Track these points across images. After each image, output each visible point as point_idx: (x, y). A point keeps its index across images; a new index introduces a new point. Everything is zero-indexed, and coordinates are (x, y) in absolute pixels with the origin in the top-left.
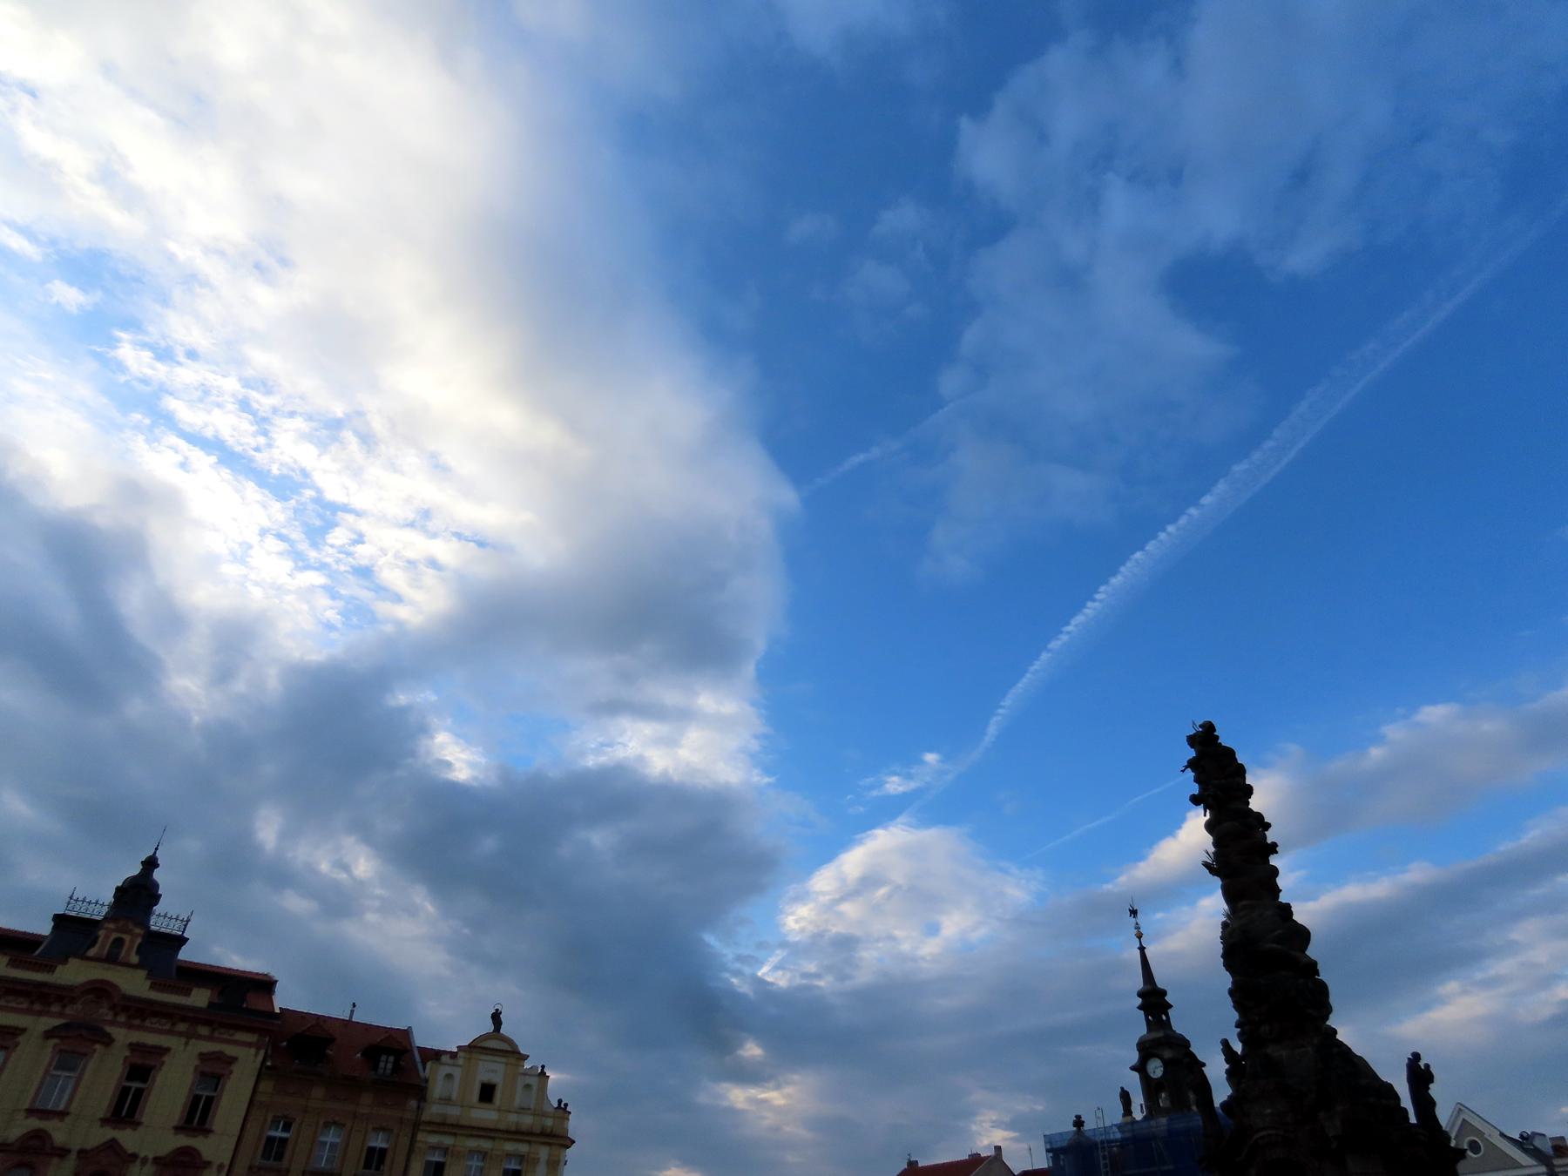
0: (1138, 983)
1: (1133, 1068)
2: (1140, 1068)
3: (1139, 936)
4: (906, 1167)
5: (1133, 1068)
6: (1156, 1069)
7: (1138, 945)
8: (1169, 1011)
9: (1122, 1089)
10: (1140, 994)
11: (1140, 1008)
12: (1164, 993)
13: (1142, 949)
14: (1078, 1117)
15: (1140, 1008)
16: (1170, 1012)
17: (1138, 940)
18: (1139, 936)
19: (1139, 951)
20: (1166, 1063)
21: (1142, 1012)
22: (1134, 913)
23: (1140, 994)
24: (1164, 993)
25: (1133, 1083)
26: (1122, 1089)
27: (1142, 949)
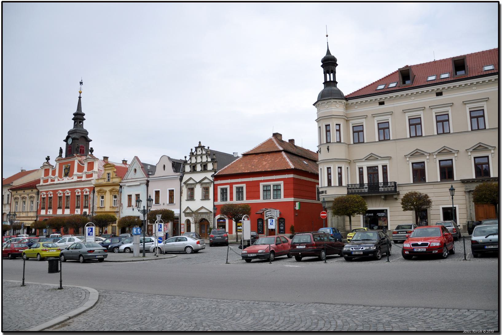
0: (75, 111)
1: (64, 141)
2: (66, 141)
3: (80, 93)
4: (21, 172)
5: (64, 141)
6: (70, 141)
7: (79, 96)
8: (84, 121)
9: (61, 148)
10: (74, 114)
11: (73, 119)
12: (84, 115)
13: (80, 97)
14: (48, 157)
15: (73, 119)
16: (84, 121)
17: (79, 94)
18: (80, 93)
19: (79, 98)
20: (73, 139)
21: (73, 121)
22: (81, 83)
23: (74, 114)
24: (84, 115)
25: (64, 146)
26: (61, 148)
27: (80, 97)
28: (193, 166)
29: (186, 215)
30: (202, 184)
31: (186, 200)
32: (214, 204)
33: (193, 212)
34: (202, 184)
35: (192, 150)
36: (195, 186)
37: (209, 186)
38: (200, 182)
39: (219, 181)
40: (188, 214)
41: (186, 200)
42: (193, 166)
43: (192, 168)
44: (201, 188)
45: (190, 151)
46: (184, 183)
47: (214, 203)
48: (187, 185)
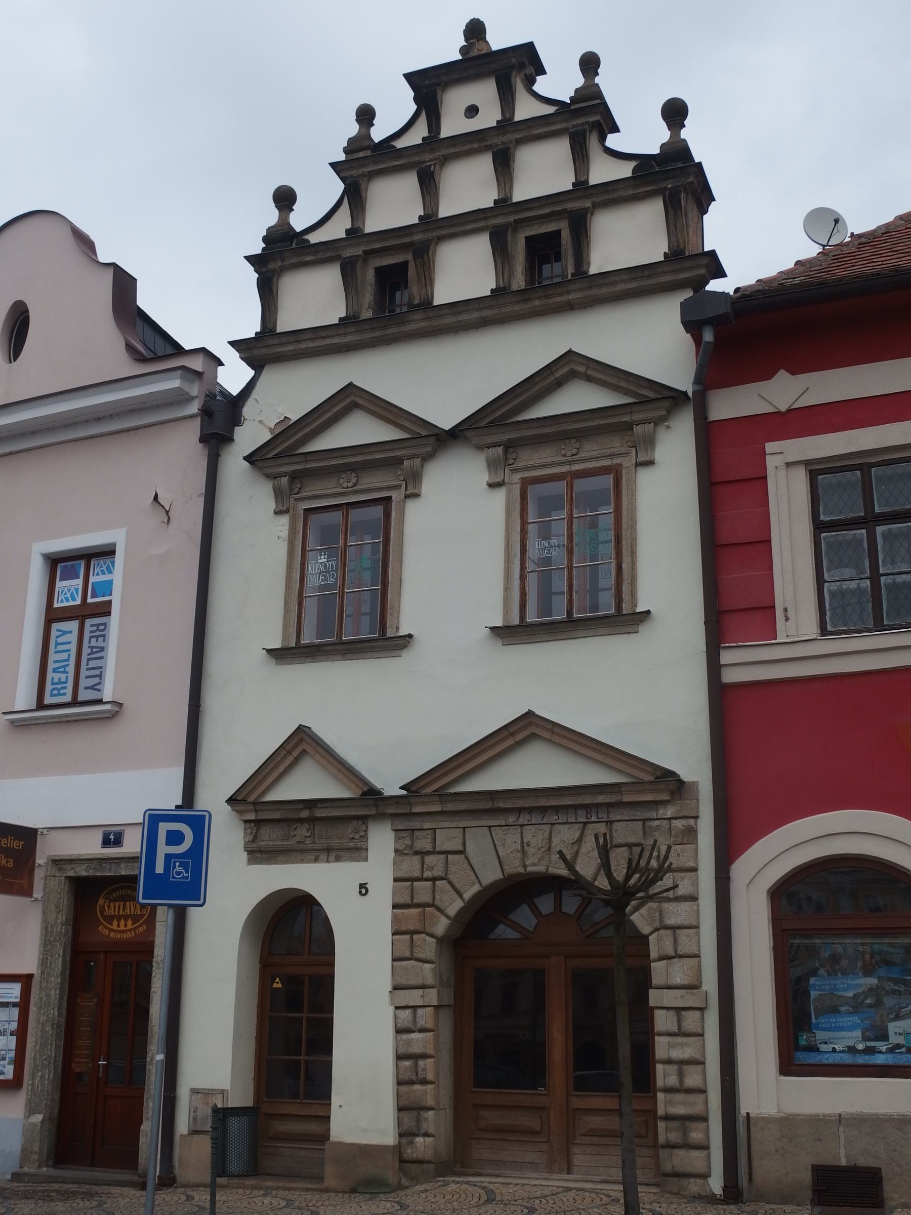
28: (379, 271)
29: (270, 837)
30: (509, 446)
31: (279, 655)
32: (714, 667)
33: (371, 794)
34: (509, 446)
35: (366, 115)
36: (415, 478)
37: (627, 462)
38: (498, 424)
39: (782, 374)
40: (302, 831)
41: (279, 655)
42: (379, 271)
43: (368, 297)
44: (500, 495)
45: (353, 129)
46: (248, 458)
47: (726, 657)
48: (294, 477)
